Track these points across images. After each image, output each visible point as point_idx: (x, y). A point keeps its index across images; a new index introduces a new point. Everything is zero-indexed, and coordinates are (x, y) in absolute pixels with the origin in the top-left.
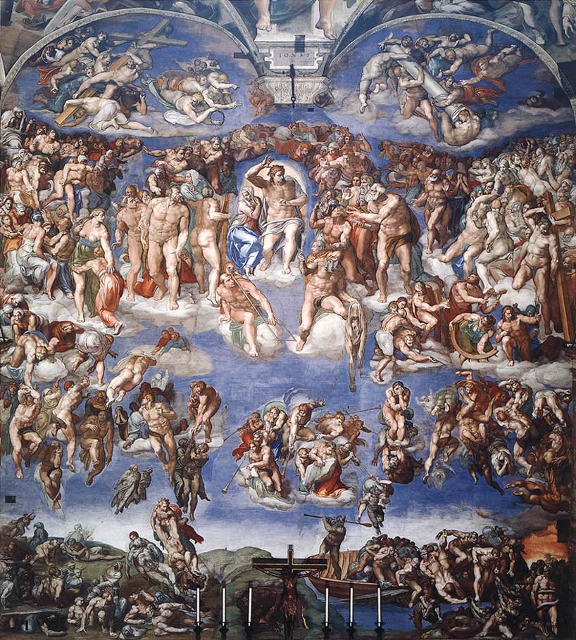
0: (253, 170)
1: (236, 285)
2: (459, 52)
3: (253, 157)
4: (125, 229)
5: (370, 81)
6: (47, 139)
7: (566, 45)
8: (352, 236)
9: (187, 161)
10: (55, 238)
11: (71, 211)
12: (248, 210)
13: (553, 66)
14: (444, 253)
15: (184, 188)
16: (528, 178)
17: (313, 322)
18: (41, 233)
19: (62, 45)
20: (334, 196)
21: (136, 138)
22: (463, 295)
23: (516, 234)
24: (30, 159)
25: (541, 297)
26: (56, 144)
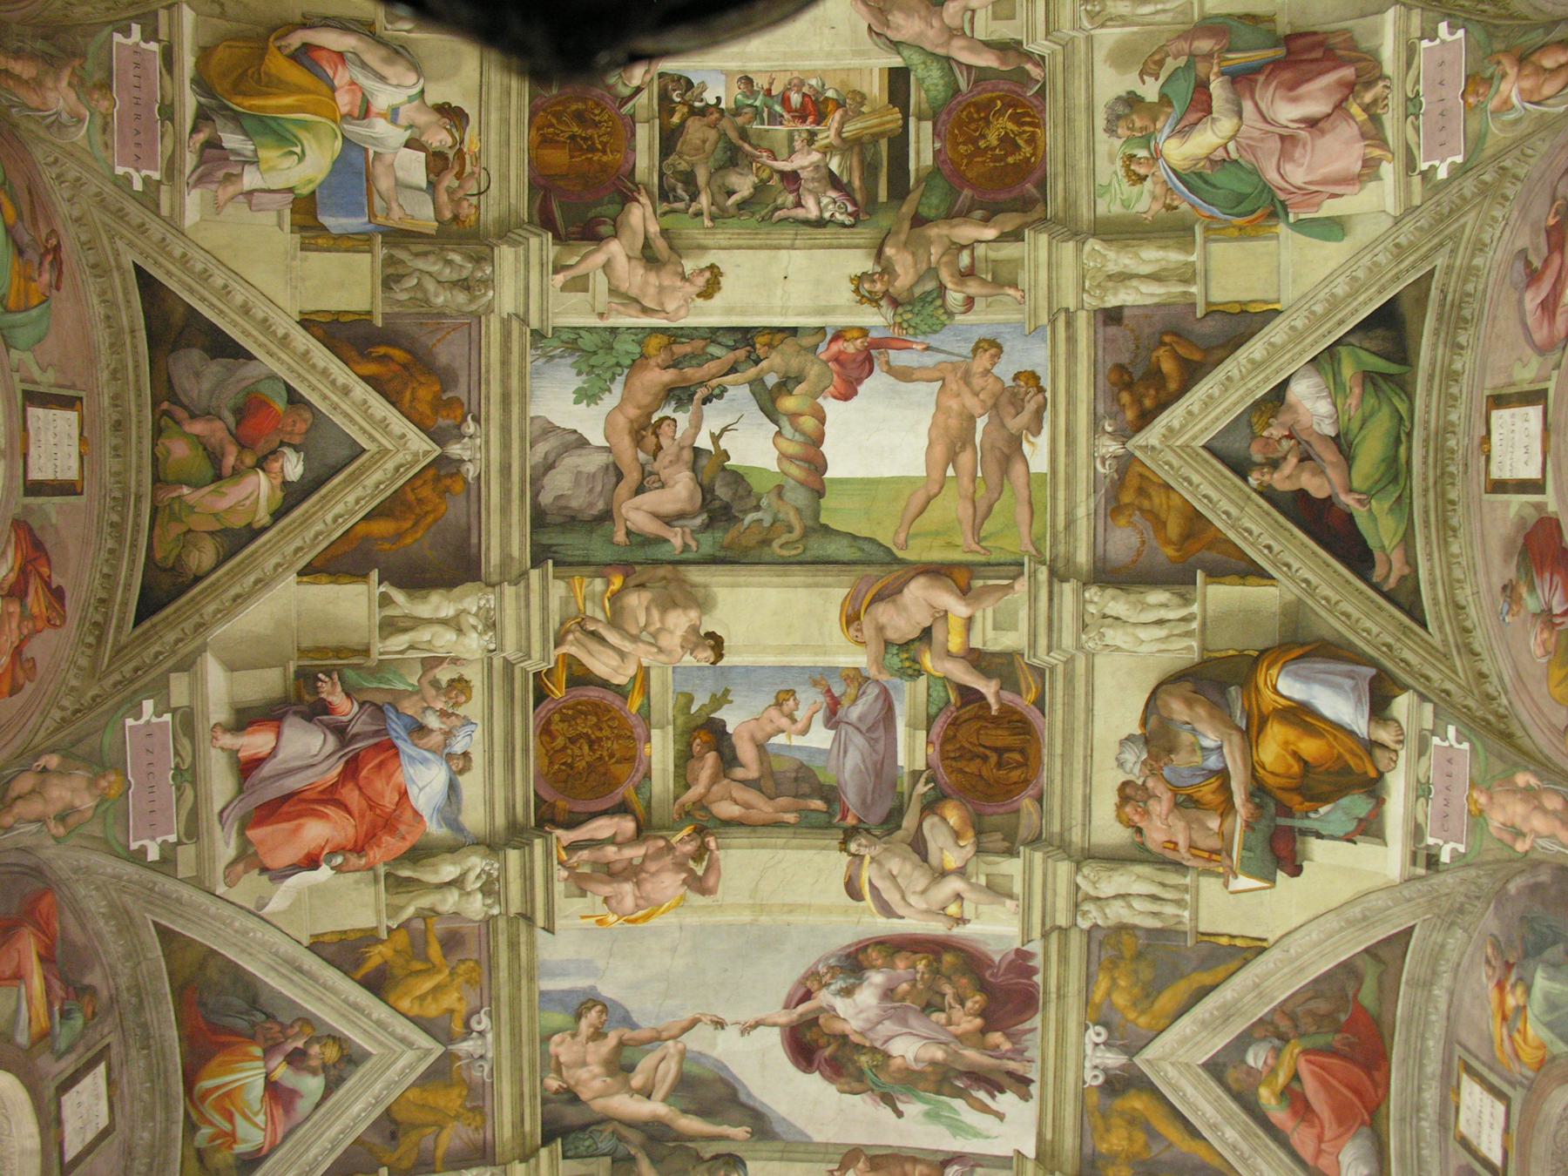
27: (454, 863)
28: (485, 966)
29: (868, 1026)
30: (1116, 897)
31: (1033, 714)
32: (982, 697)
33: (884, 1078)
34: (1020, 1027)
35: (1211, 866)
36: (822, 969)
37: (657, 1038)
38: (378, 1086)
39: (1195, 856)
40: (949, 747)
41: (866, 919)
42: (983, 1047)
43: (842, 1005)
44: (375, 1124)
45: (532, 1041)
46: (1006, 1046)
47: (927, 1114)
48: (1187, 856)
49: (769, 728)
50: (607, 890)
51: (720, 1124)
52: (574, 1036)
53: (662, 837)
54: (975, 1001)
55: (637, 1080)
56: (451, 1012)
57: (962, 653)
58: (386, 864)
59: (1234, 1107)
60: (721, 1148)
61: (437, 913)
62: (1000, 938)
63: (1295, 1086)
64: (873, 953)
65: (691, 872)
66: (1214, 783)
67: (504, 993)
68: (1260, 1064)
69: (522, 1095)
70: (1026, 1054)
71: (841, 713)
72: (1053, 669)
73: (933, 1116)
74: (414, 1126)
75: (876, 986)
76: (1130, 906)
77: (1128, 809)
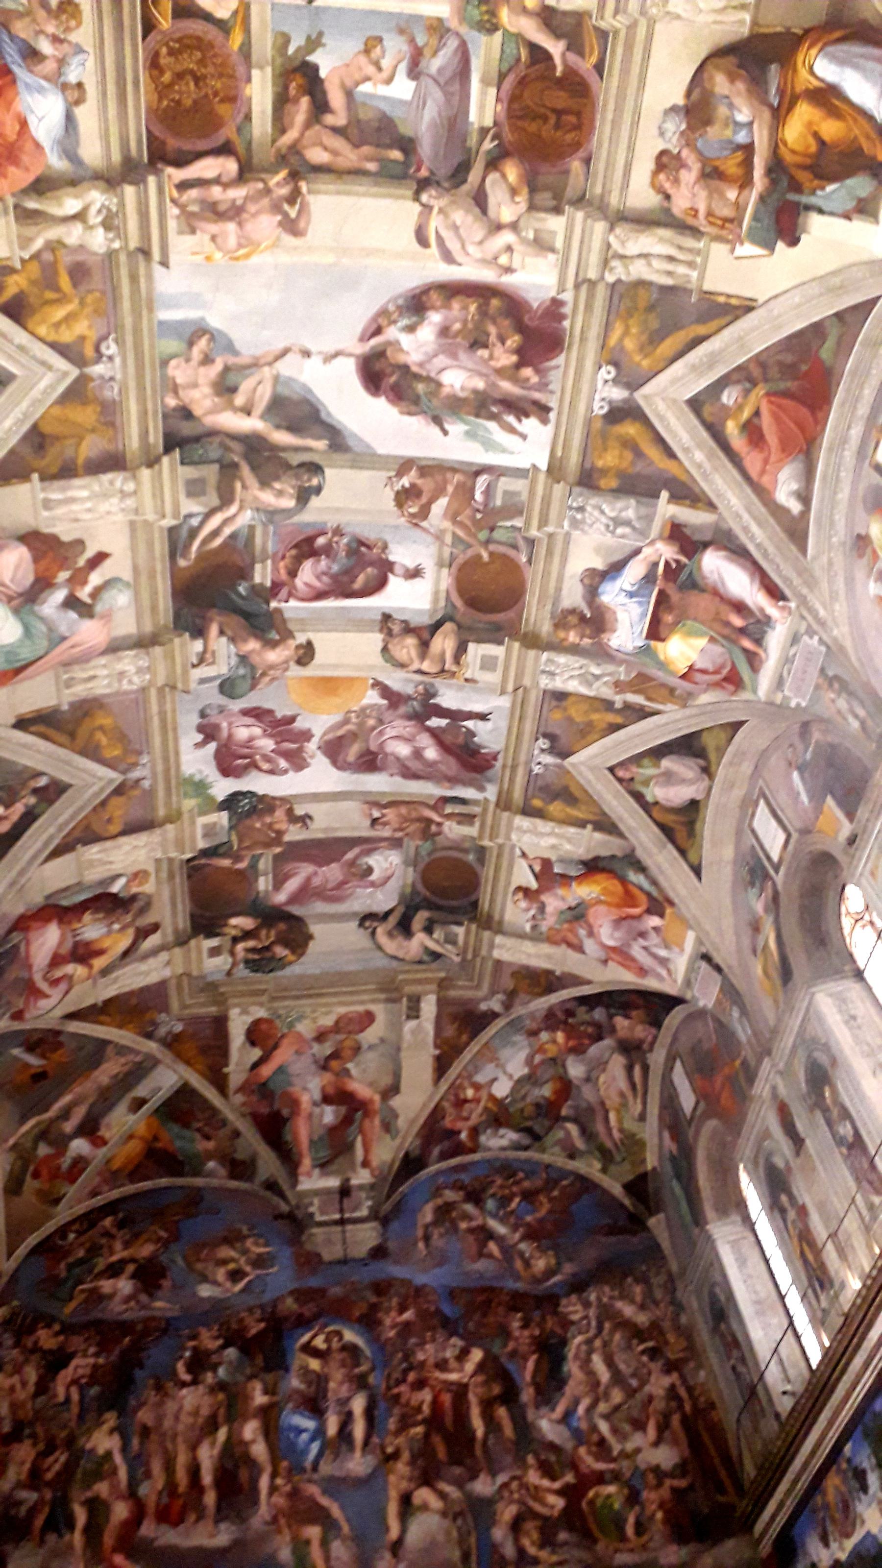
0: (306, 1338)
1: (294, 1494)
2: (515, 1189)
3: (303, 1322)
4: (145, 1432)
5: (427, 1227)
6: (50, 1332)
7: (624, 1160)
8: (436, 1403)
9: (226, 1339)
10: (51, 1459)
11: (75, 1417)
12: (302, 1387)
13: (617, 1190)
14: (553, 1410)
15: (221, 1372)
16: (628, 1310)
17: (404, 1530)
18: (32, 1454)
19: (76, 1227)
20: (406, 1357)
21: (160, 1319)
22: (591, 1463)
23: (634, 1375)
24: (26, 1361)
25: (687, 1453)
26: (61, 1338)
27: (76, 197)
28: (109, 295)
30: (640, 256)
31: (592, 78)
32: (547, 57)
35: (724, 233)
36: (391, 308)
37: (255, 365)
38: (24, 405)
39: (711, 223)
40: (516, 106)
43: (406, 340)
44: (25, 438)
46: (535, 379)
48: (704, 222)
49: (357, 76)
50: (214, 228)
52: (188, 360)
53: (263, 180)
54: (514, 340)
55: (240, 400)
56: (82, 339)
57: (537, 9)
58: (13, 195)
59: (704, 434)
60: (306, 457)
61: (64, 246)
62: (540, 287)
63: (756, 421)
64: (434, 296)
65: (286, 215)
66: (740, 156)
67: (128, 321)
68: (731, 403)
69: (145, 413)
70: (551, 387)
71: (423, 64)
72: (616, 32)
73: (471, 435)
74: (57, 438)
76: (649, 264)
77: (662, 177)
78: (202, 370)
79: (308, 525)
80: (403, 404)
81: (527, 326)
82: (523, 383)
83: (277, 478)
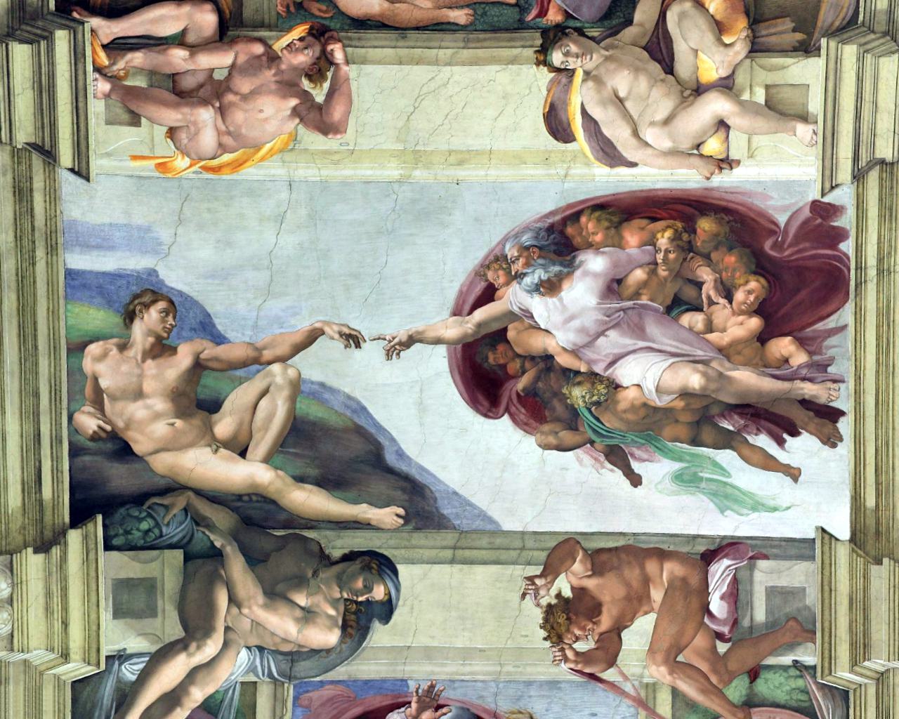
29: (587, 339)
33: (609, 421)
34: (820, 326)
36: (511, 251)
37: (256, 361)
41: (578, 170)
42: (763, 365)
43: (540, 308)
45: (54, 349)
46: (800, 359)
47: (679, 478)
51: (356, 502)
52: (123, 347)
54: (750, 289)
55: (224, 426)
60: (359, 541)
62: (787, 186)
64: (589, 224)
73: (687, 480)
75: (595, 275)
78: (149, 362)
79: (366, 682)
80: (546, 428)
81: (770, 258)
82: (780, 370)
83: (300, 582)
